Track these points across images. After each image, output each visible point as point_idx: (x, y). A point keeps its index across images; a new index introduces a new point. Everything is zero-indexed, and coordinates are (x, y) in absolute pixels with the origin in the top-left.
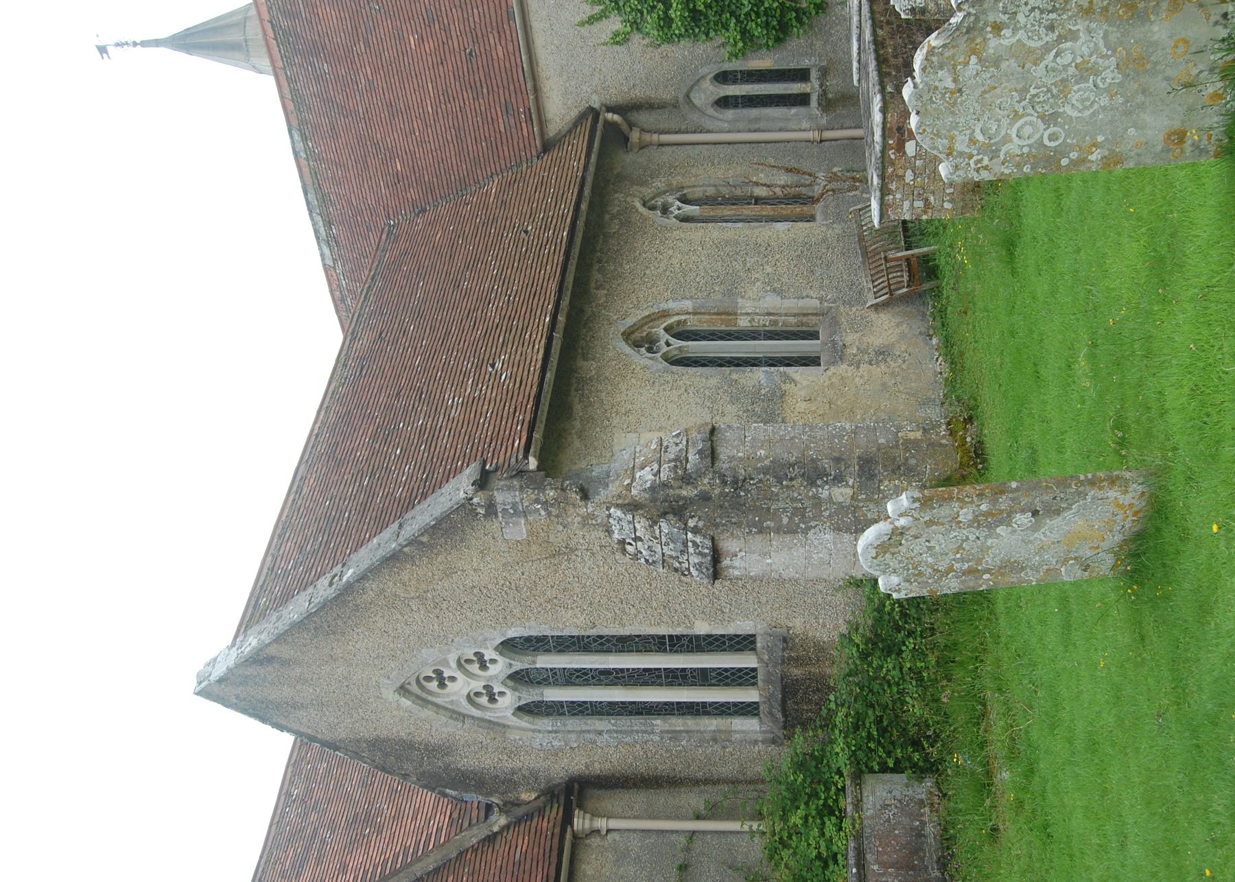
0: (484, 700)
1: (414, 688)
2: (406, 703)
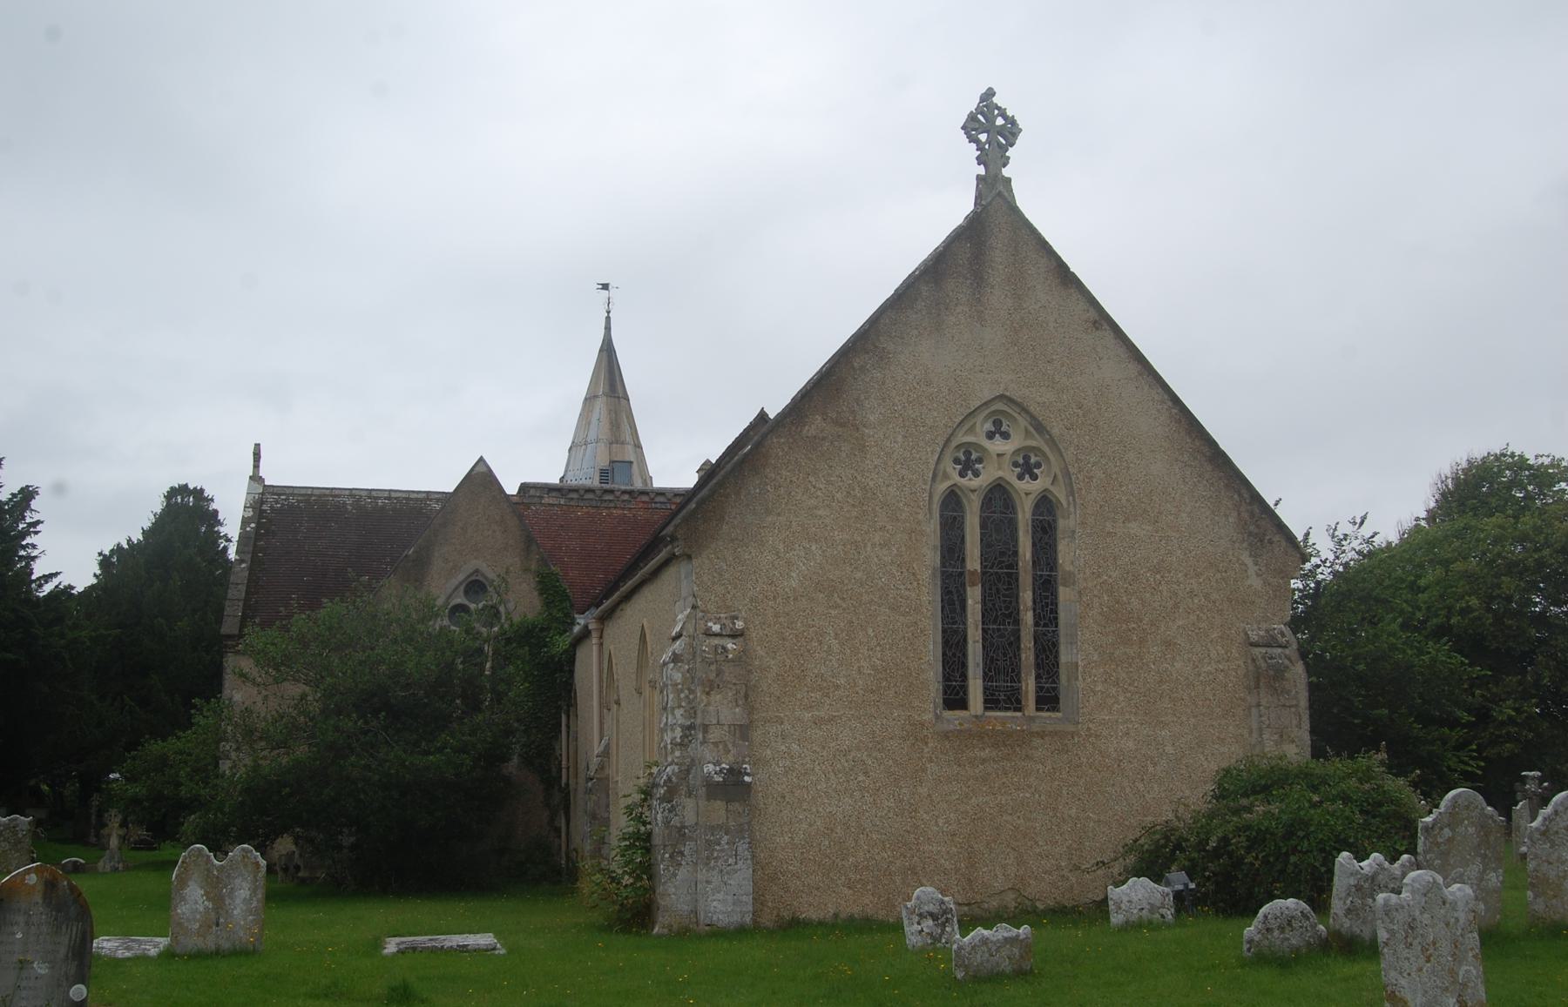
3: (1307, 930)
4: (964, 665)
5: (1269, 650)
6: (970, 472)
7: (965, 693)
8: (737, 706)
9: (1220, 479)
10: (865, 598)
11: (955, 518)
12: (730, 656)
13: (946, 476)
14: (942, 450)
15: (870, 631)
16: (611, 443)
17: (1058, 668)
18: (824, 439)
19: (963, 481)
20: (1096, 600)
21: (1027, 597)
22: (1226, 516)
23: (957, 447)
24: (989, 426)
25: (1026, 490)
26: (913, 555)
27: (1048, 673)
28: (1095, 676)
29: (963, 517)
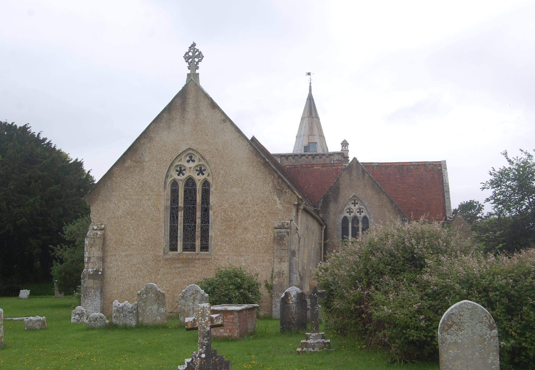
0: (348, 211)
1: (354, 198)
2: (351, 197)
4: (177, 237)
5: (281, 230)
6: (181, 174)
7: (177, 246)
8: (99, 251)
9: (267, 171)
11: (176, 189)
12: (98, 236)
13: (171, 176)
14: (169, 168)
15: (144, 227)
16: (309, 136)
18: (131, 167)
19: (178, 177)
20: (219, 215)
21: (198, 214)
22: (269, 184)
23: (176, 166)
24: (188, 158)
25: (199, 179)
28: (218, 240)
29: (178, 189)
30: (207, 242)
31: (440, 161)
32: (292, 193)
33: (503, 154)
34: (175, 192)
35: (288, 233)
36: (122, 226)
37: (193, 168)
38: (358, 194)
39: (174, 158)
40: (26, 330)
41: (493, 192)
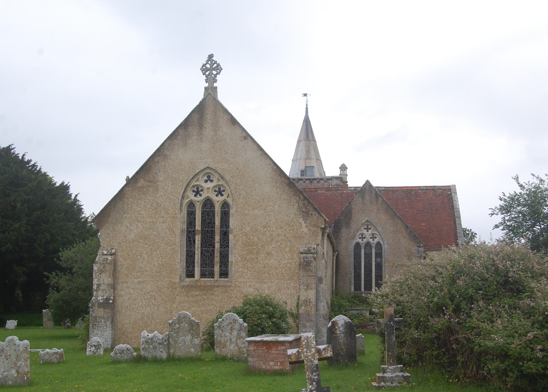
1: (366, 223)
3: (129, 354)
4: (194, 262)
5: (307, 255)
6: (198, 195)
7: (194, 272)
8: (110, 278)
9: (292, 192)
10: (157, 241)
11: (193, 211)
12: (108, 262)
13: (188, 197)
16: (306, 159)
17: (228, 263)
18: (144, 187)
19: (196, 199)
20: (240, 238)
21: (217, 238)
24: (206, 178)
25: (218, 200)
26: (174, 225)
27: (225, 265)
28: (239, 266)
29: (195, 211)
30: (226, 268)
31: (450, 185)
32: (319, 215)
33: (515, 179)
34: (192, 214)
35: (315, 259)
36: (134, 250)
37: (211, 189)
38: (371, 219)
39: (191, 177)
40: (42, 364)
41: (502, 218)
